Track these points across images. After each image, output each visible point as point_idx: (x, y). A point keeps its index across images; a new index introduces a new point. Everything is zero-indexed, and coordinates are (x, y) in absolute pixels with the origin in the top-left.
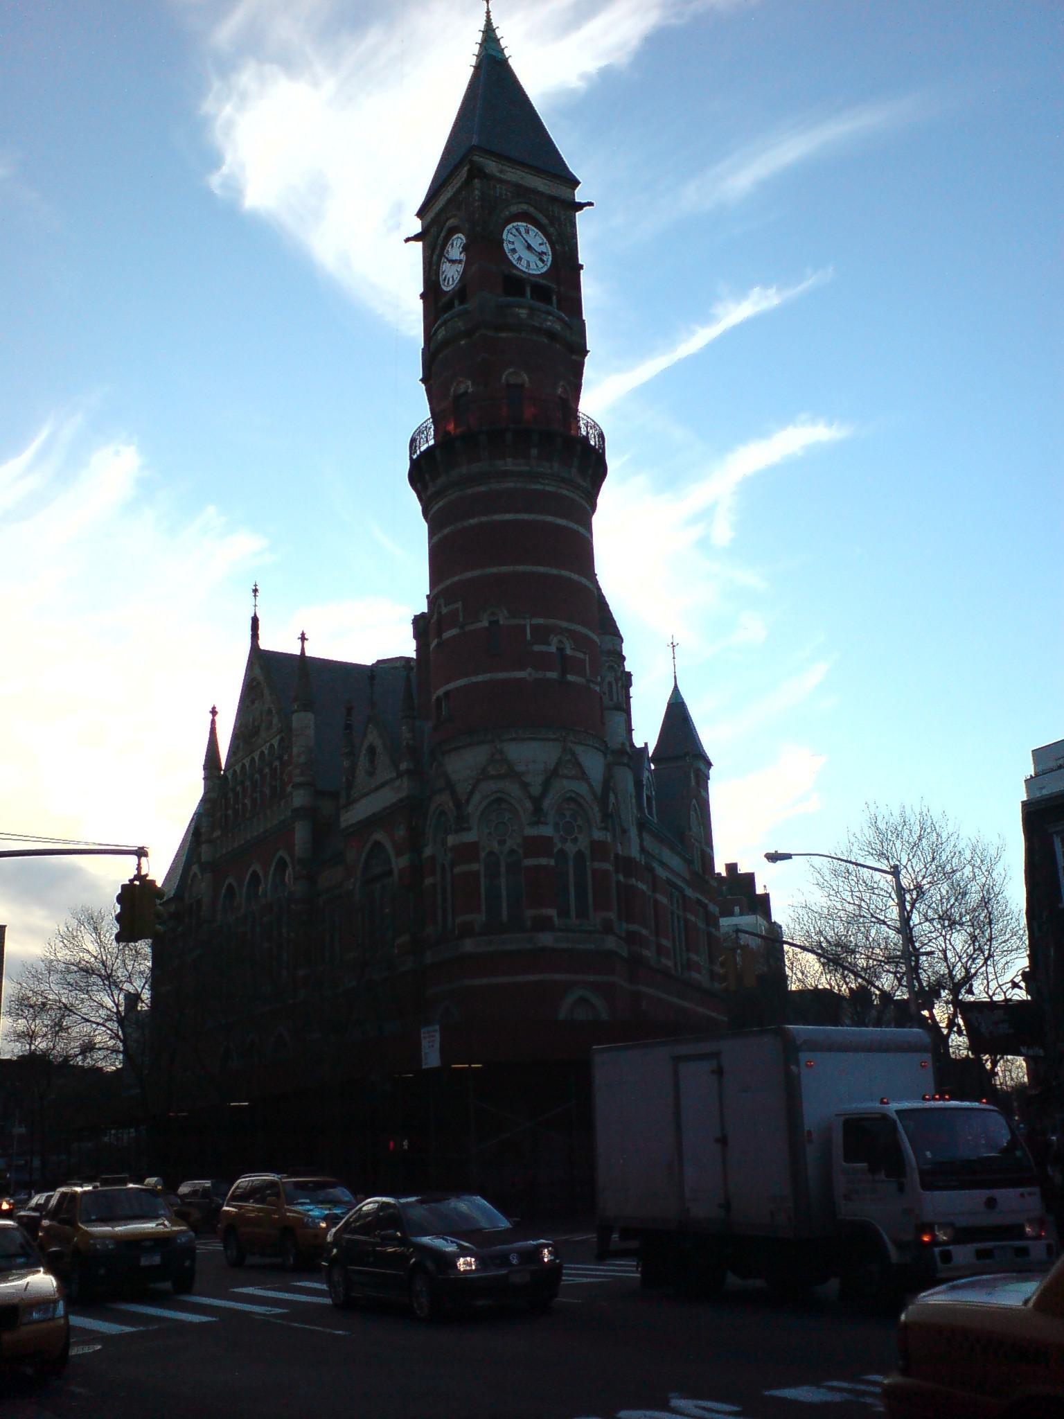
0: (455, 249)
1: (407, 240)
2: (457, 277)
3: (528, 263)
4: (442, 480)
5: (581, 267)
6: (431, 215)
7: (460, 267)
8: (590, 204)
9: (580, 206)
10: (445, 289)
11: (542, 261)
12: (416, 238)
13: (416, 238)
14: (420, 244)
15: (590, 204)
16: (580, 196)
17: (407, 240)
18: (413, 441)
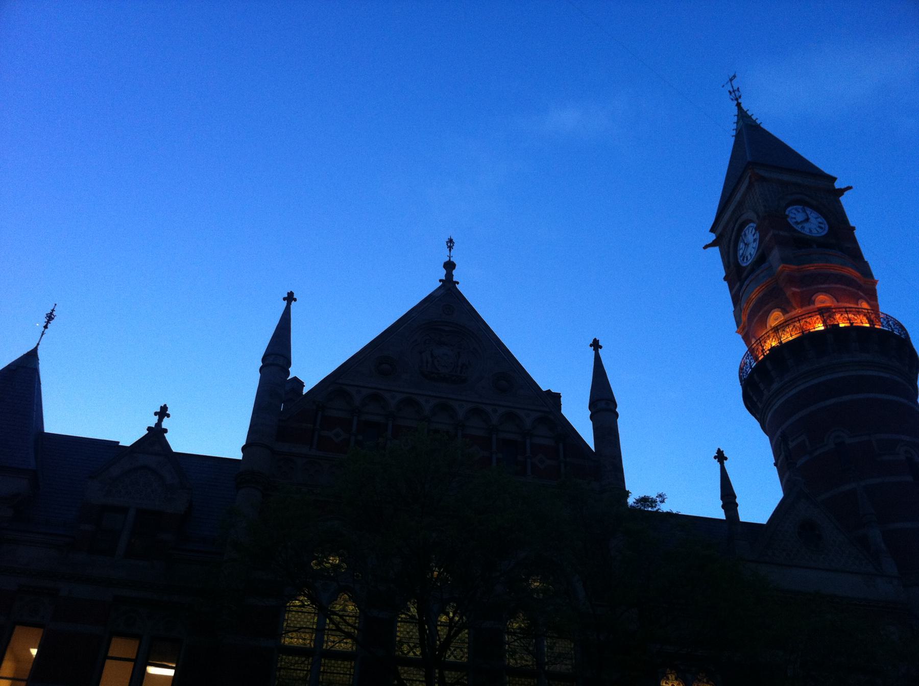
0: (751, 235)
1: (706, 247)
2: (753, 252)
3: (811, 231)
4: (775, 386)
5: (853, 228)
6: (720, 229)
7: (755, 245)
8: (849, 188)
9: (841, 192)
10: (744, 265)
11: (821, 228)
12: (713, 244)
13: (713, 244)
14: (716, 250)
15: (849, 188)
16: (838, 185)
17: (706, 247)
18: (741, 369)
